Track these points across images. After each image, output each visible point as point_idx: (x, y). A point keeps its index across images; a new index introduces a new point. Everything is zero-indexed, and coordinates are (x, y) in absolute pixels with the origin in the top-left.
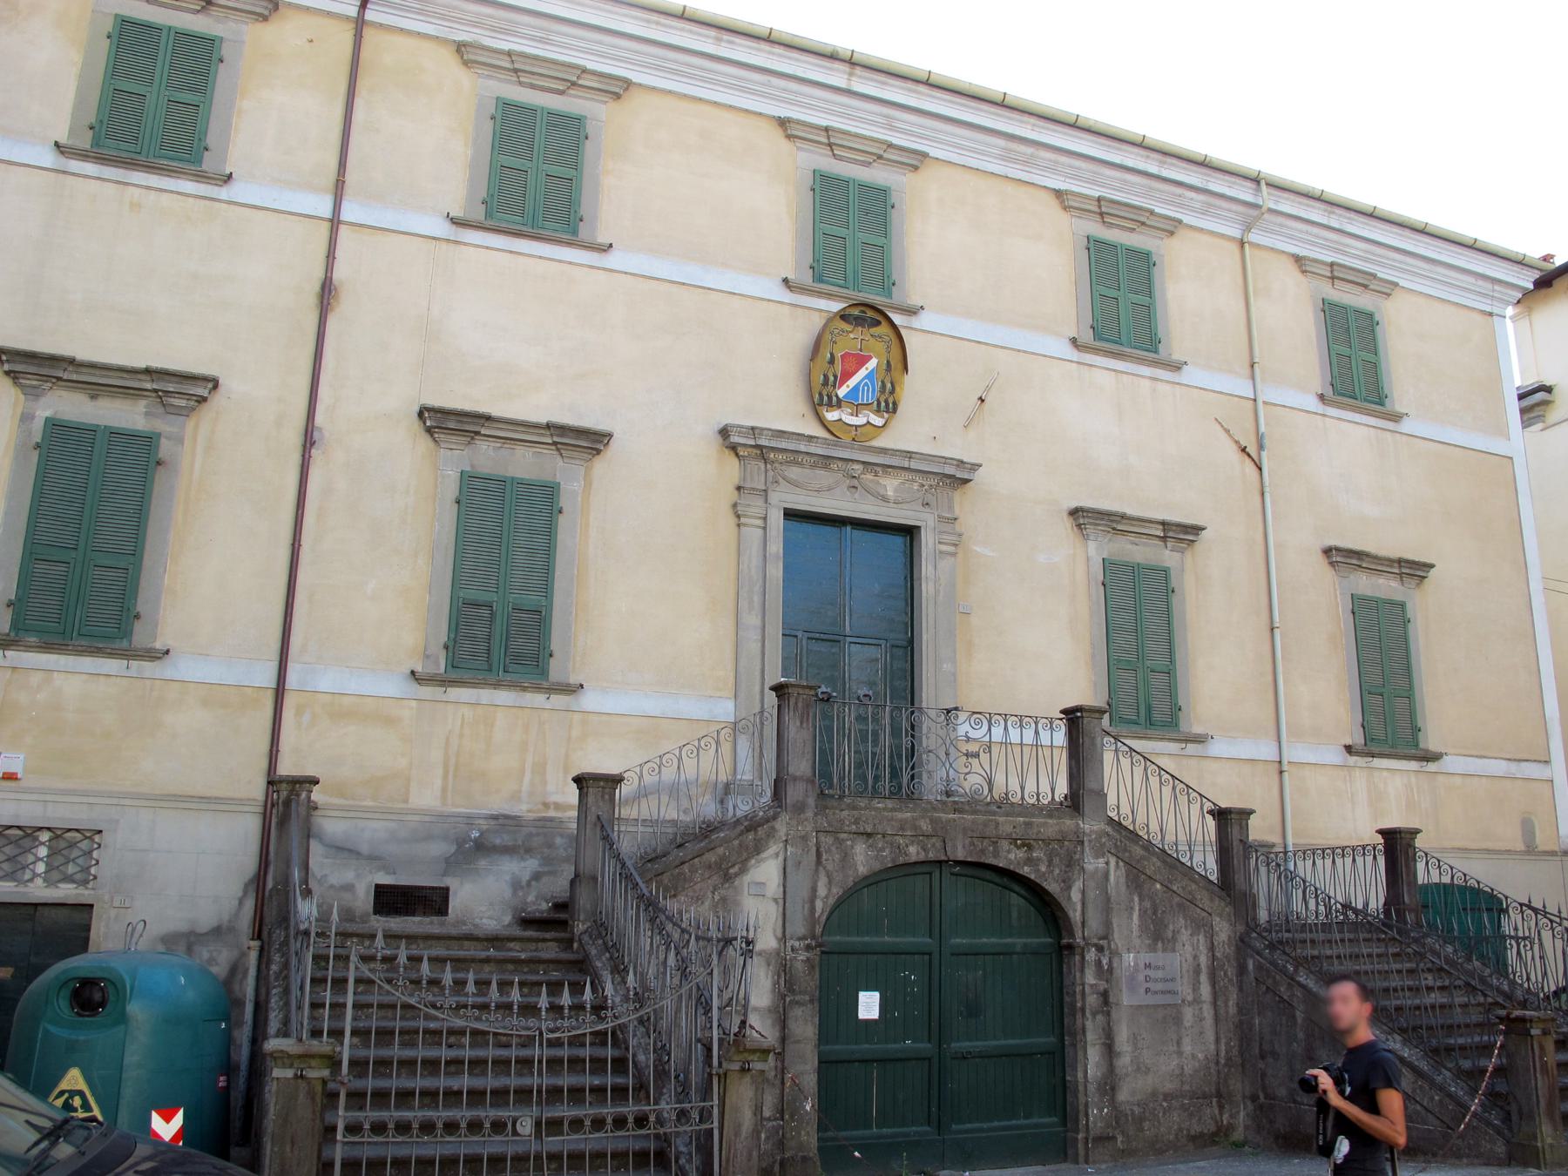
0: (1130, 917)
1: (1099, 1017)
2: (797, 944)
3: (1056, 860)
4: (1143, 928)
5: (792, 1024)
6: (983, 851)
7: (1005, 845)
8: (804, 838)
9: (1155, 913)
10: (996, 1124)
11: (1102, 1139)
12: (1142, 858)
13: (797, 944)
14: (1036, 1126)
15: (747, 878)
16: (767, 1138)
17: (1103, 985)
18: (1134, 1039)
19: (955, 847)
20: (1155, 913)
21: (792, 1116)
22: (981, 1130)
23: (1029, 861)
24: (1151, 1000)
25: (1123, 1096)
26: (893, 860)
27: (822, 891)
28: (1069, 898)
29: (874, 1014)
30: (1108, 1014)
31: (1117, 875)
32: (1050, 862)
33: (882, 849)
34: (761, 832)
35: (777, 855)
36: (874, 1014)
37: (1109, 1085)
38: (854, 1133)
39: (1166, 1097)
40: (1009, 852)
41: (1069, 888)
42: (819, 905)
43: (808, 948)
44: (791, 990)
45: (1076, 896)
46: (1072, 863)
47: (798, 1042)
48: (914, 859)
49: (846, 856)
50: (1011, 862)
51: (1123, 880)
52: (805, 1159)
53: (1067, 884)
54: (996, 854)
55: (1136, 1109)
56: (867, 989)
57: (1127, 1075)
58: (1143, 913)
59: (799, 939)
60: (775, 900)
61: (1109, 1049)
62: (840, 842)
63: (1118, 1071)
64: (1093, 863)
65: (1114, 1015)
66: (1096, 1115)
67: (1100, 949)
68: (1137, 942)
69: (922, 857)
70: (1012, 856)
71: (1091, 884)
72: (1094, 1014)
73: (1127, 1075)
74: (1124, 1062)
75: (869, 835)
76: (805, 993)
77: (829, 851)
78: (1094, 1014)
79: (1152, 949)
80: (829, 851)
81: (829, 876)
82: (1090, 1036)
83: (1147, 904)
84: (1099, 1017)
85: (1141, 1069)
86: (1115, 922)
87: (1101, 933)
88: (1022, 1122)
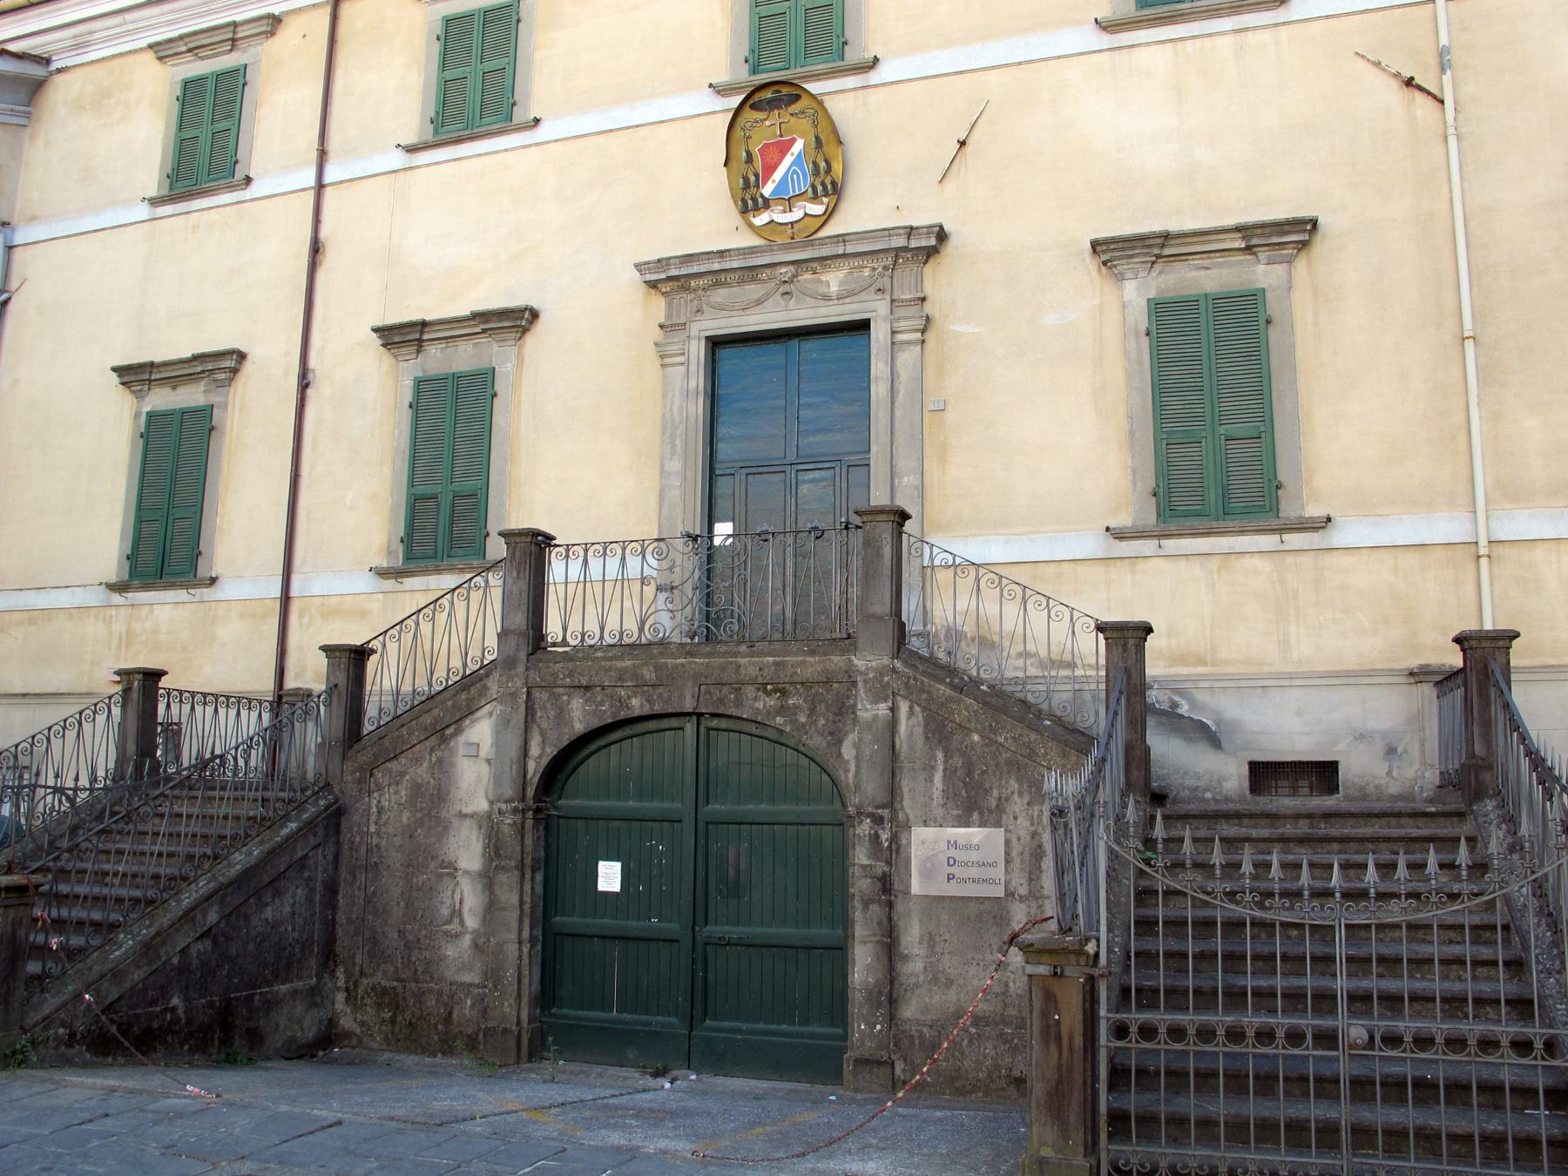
0: (930, 780)
1: (874, 908)
2: (504, 806)
3: (821, 708)
4: (949, 794)
5: (497, 890)
6: (721, 700)
7: (750, 691)
8: (514, 695)
9: (969, 773)
10: (761, 1026)
11: (863, 1062)
12: (950, 699)
13: (504, 806)
14: (812, 1036)
15: (462, 739)
16: (473, 1005)
17: (881, 867)
18: (930, 940)
19: (682, 696)
20: (969, 773)
21: (495, 986)
22: (740, 1031)
23: (782, 710)
24: (953, 890)
25: (910, 1011)
26: (614, 715)
27: (535, 750)
28: (840, 755)
29: (615, 886)
30: (890, 905)
31: (909, 725)
32: (812, 711)
33: (601, 703)
34: (473, 690)
35: (491, 714)
36: (615, 886)
37: (889, 995)
38: (580, 1013)
39: (977, 1020)
40: (756, 699)
41: (840, 742)
42: (531, 765)
43: (515, 811)
44: (497, 855)
45: (848, 751)
46: (843, 711)
47: (504, 909)
48: (636, 713)
49: (562, 715)
50: (758, 711)
51: (919, 730)
52: (505, 1030)
53: (837, 739)
54: (738, 703)
55: (925, 1030)
56: (607, 859)
57: (916, 985)
58: (949, 774)
59: (506, 802)
60: (488, 761)
61: (890, 948)
62: (557, 697)
63: (903, 979)
64: (870, 710)
65: (900, 906)
66: (863, 1030)
67: (878, 821)
68: (940, 812)
69: (646, 710)
70: (759, 705)
71: (869, 737)
72: (866, 904)
73: (916, 985)
74: (913, 968)
75: (587, 688)
76: (511, 858)
77: (543, 708)
78: (866, 904)
79: (964, 822)
80: (543, 708)
81: (542, 734)
82: (859, 931)
83: (958, 761)
84: (874, 908)
85: (937, 978)
86: (906, 785)
87: (879, 799)
88: (797, 1028)
